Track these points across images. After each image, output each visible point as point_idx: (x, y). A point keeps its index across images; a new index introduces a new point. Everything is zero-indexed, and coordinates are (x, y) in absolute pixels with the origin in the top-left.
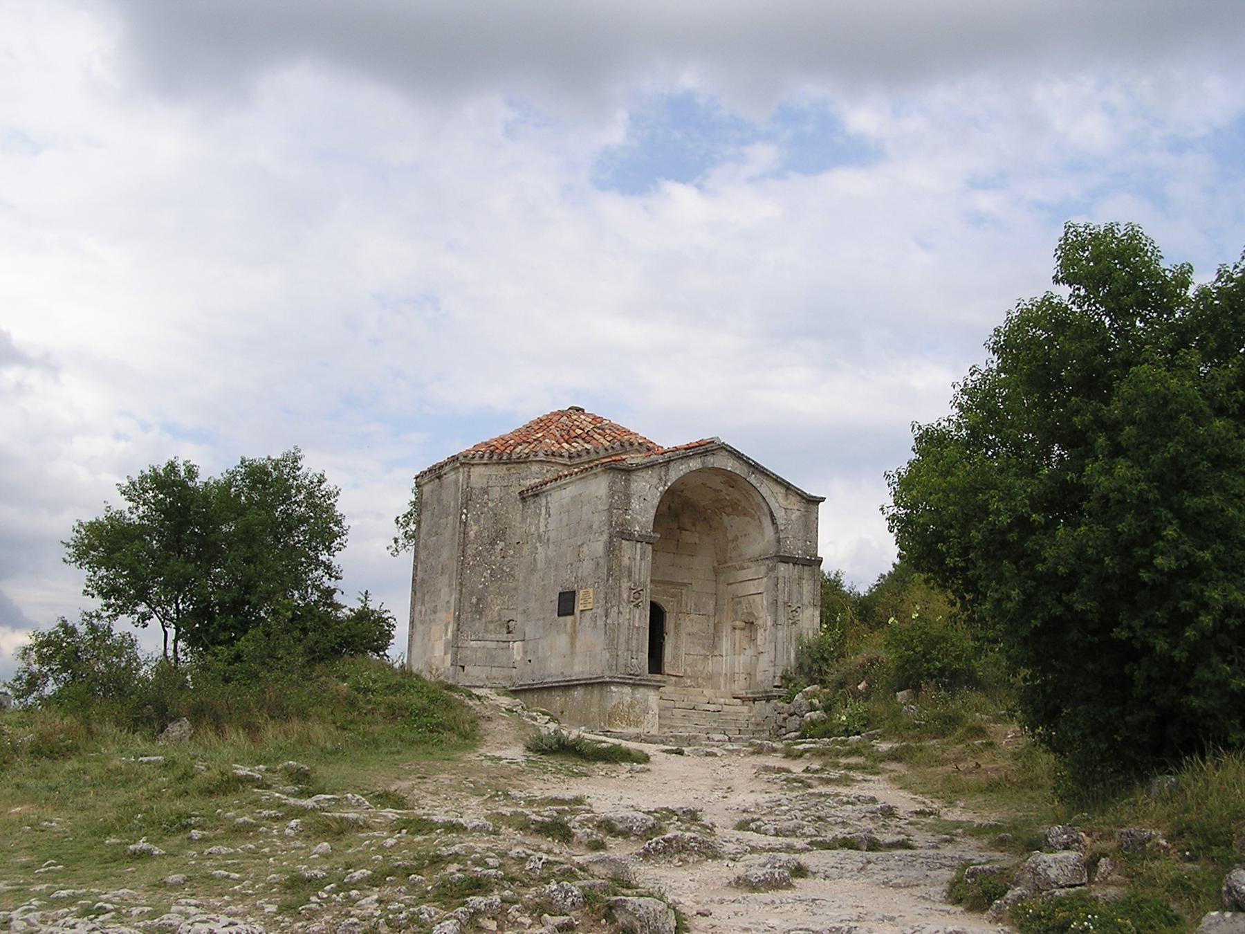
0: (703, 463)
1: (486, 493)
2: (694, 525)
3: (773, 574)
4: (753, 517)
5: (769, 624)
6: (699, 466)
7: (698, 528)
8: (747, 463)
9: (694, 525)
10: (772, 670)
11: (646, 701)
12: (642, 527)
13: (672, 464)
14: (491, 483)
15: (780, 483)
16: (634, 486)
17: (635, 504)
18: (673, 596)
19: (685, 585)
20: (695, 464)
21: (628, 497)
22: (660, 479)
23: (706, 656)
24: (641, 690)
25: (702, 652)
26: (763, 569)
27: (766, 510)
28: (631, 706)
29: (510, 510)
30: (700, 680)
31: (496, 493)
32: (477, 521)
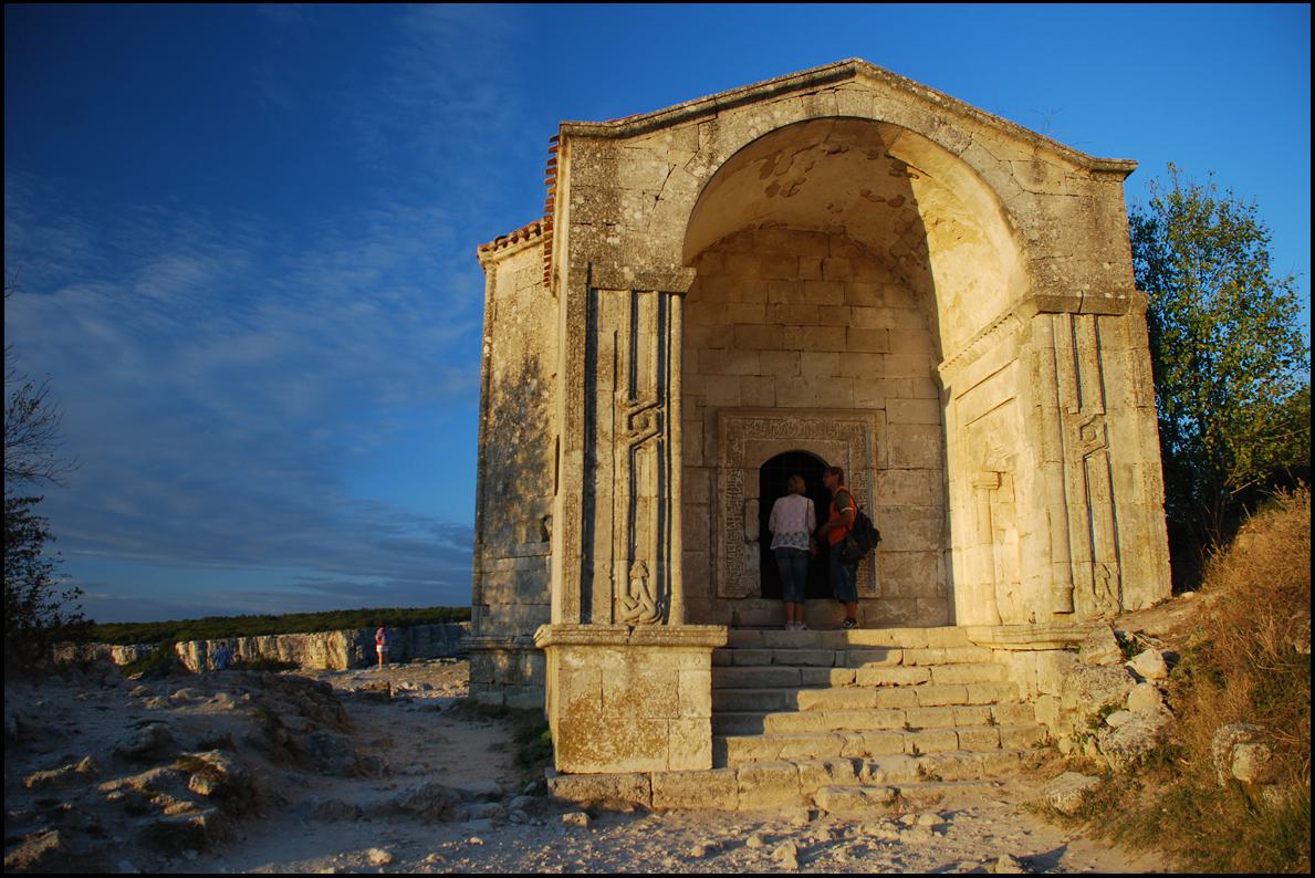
0: (810, 108)
1: (513, 301)
2: (882, 296)
3: (1027, 349)
4: (973, 238)
5: (1032, 464)
6: (797, 117)
7: (890, 300)
8: (923, 99)
9: (882, 296)
10: (1046, 572)
11: (674, 685)
12: (654, 260)
13: (724, 116)
14: (520, 286)
15: (1014, 137)
16: (625, 171)
17: (632, 210)
18: (844, 437)
19: (870, 411)
20: (788, 111)
21: (612, 196)
22: (697, 151)
23: (929, 552)
24: (655, 655)
25: (922, 544)
26: (1010, 341)
27: (992, 207)
28: (630, 699)
29: (543, 322)
30: (921, 603)
31: (527, 297)
32: (503, 353)
